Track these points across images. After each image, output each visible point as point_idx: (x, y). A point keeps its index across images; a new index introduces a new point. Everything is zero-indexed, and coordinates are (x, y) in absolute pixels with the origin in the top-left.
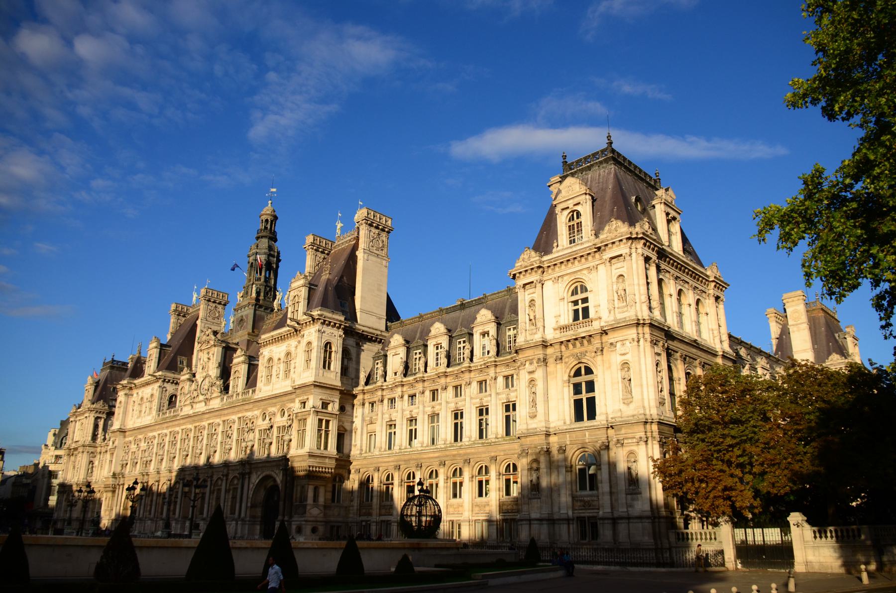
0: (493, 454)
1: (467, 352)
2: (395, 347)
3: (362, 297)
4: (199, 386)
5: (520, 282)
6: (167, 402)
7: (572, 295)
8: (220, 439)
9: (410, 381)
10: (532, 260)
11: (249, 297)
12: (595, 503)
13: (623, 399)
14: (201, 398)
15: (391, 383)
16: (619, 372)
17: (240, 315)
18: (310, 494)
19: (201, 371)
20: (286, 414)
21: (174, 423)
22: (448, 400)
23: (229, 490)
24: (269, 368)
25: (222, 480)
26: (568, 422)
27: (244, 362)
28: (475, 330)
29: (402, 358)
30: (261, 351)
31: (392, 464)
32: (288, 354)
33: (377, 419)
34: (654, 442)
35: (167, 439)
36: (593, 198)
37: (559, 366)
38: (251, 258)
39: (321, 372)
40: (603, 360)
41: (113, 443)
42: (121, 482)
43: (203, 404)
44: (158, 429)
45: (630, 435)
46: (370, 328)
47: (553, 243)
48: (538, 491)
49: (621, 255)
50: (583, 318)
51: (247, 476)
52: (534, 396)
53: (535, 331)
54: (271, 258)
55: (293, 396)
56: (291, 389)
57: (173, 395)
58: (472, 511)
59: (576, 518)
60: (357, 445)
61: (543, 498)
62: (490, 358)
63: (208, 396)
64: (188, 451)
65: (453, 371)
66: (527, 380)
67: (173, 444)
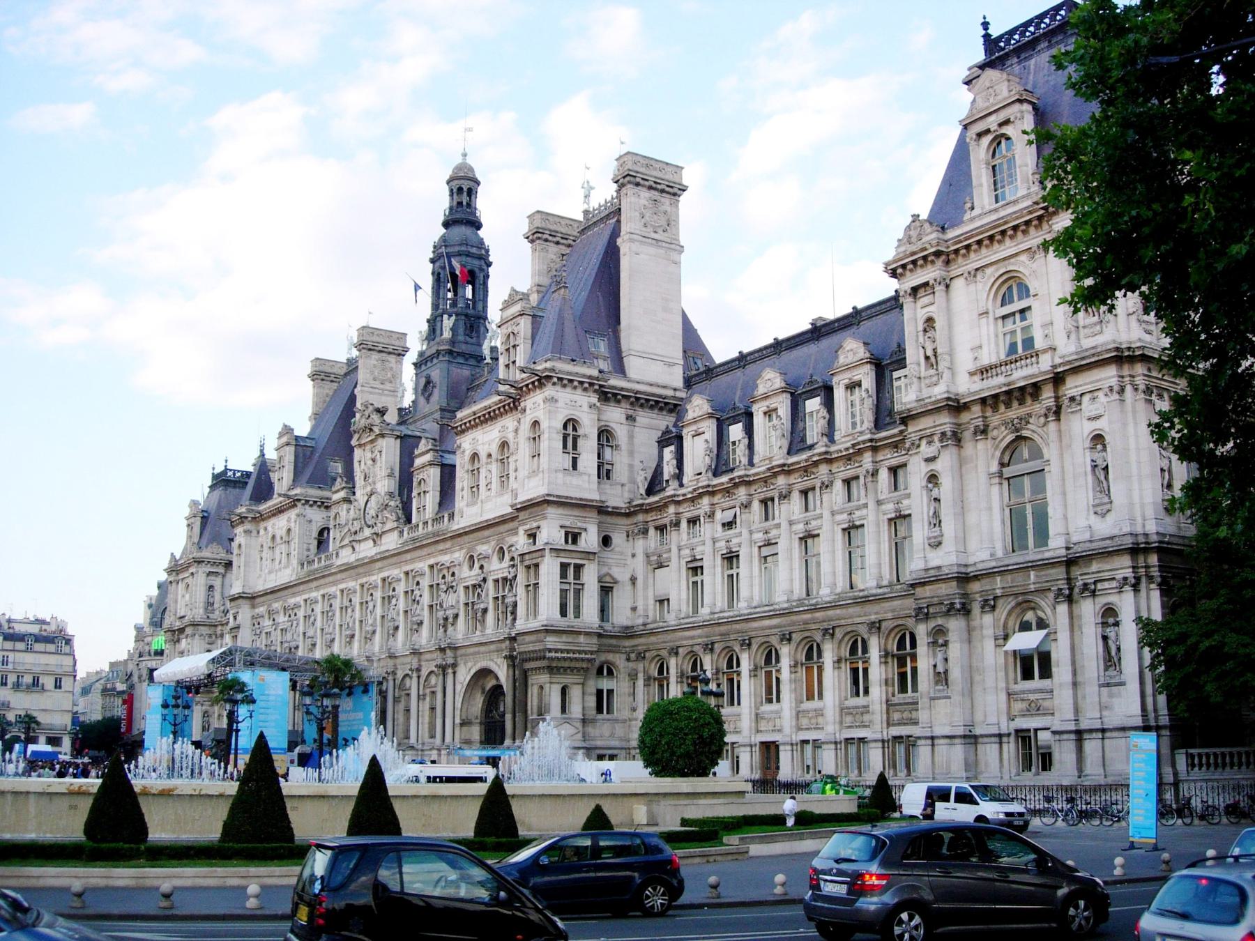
0: (873, 618)
2: (695, 421)
6: (316, 543)
8: (402, 605)
9: (723, 484)
10: (925, 239)
11: (437, 339)
12: (1046, 704)
13: (1093, 506)
14: (367, 532)
15: (690, 489)
16: (1088, 453)
17: (425, 373)
18: (555, 700)
19: (363, 483)
20: (507, 557)
22: (793, 518)
23: (424, 695)
24: (474, 472)
25: (411, 678)
26: (1000, 554)
27: (431, 464)
28: (835, 380)
29: (706, 441)
30: (458, 442)
31: (700, 641)
32: (504, 445)
33: (669, 560)
34: (1153, 586)
35: (318, 608)
36: (1035, 108)
37: (980, 445)
39: (560, 475)
40: (1060, 431)
41: (235, 618)
43: (371, 542)
45: (1106, 575)
46: (651, 385)
48: (947, 684)
50: (1024, 350)
51: (450, 671)
52: (937, 504)
53: (935, 379)
55: (515, 524)
56: (509, 510)
57: (324, 528)
58: (841, 723)
59: (1013, 732)
61: (956, 698)
63: (378, 529)
65: (799, 463)
66: (923, 475)
67: (328, 614)
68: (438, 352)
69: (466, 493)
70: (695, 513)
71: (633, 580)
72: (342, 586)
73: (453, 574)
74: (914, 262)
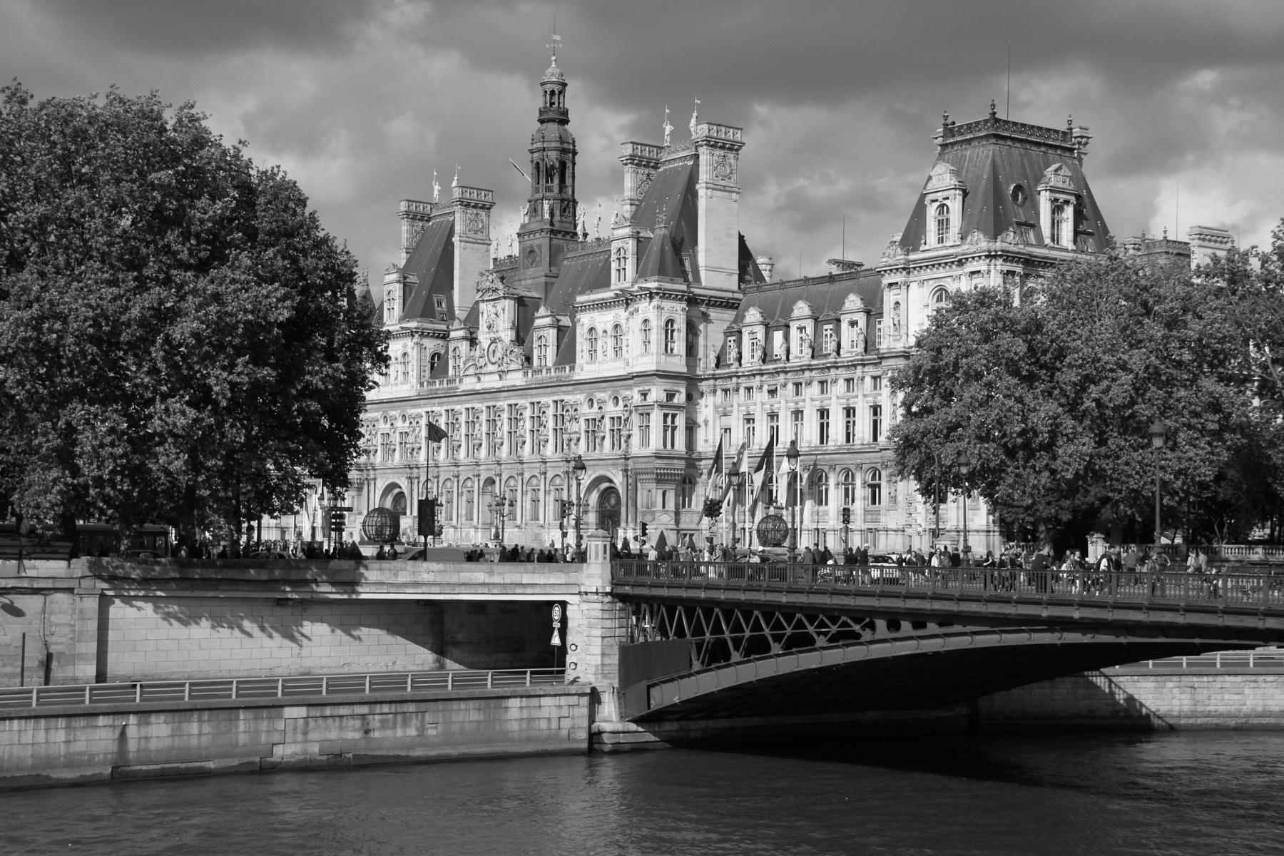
3: (707, 251)
5: (887, 280)
7: (937, 301)
10: (898, 258)
11: (539, 218)
14: (491, 368)
17: (528, 244)
20: (621, 401)
21: (451, 399)
24: (593, 341)
27: (551, 326)
33: (732, 412)
39: (663, 357)
42: (372, 476)
43: (496, 377)
44: (425, 405)
46: (718, 290)
49: (979, 272)
62: (857, 355)
63: (504, 368)
68: (542, 230)
69: (586, 355)
70: (750, 385)
71: (706, 422)
72: (469, 406)
73: (576, 410)
74: (891, 270)
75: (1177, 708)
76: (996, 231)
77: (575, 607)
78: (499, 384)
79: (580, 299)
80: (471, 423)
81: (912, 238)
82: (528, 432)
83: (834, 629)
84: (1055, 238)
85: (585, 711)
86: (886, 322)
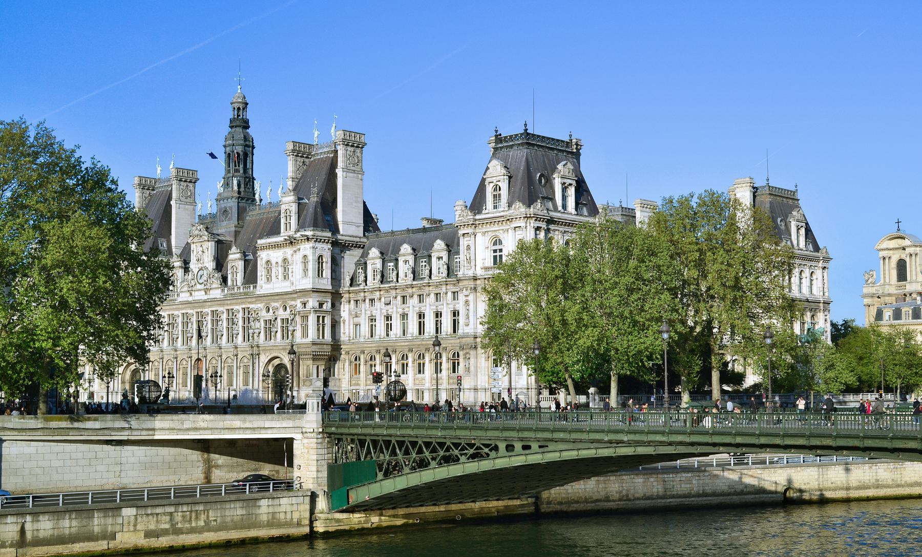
1: (427, 272)
2: (373, 259)
4: (195, 276)
7: (494, 245)
10: (469, 217)
14: (199, 287)
21: (171, 307)
24: (269, 271)
27: (240, 259)
31: (375, 348)
32: (285, 260)
33: (361, 314)
38: (228, 149)
39: (317, 279)
43: (203, 293)
47: (483, 206)
51: (257, 357)
54: (248, 149)
60: (346, 332)
62: (443, 278)
63: (208, 286)
64: (192, 334)
65: (417, 284)
68: (232, 197)
70: (373, 297)
72: (184, 311)
75: (655, 494)
76: (529, 203)
77: (298, 442)
78: (205, 297)
79: (259, 242)
80: (186, 324)
81: (477, 205)
82: (225, 328)
83: (472, 451)
84: (564, 206)
85: (308, 507)
86: (462, 257)
